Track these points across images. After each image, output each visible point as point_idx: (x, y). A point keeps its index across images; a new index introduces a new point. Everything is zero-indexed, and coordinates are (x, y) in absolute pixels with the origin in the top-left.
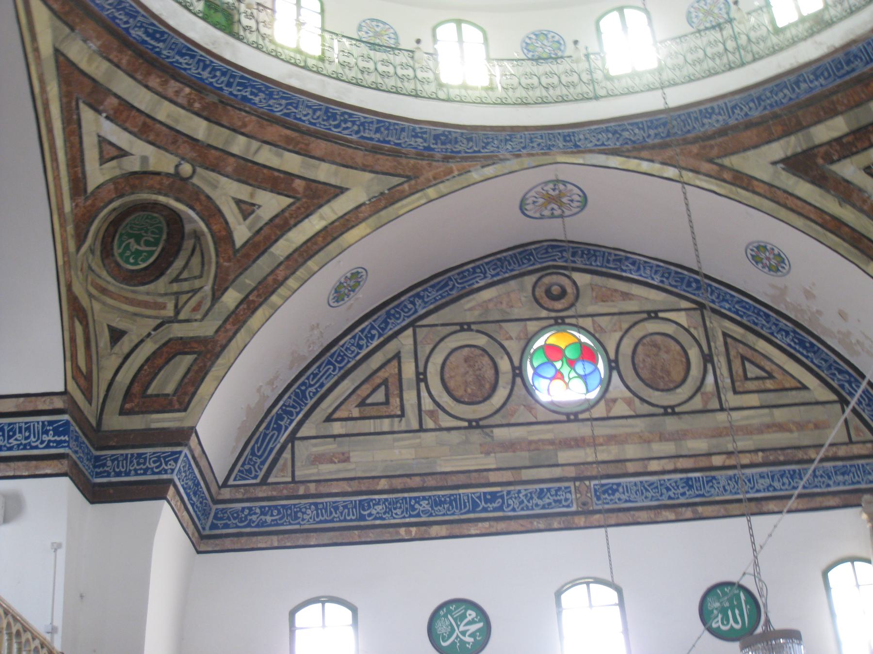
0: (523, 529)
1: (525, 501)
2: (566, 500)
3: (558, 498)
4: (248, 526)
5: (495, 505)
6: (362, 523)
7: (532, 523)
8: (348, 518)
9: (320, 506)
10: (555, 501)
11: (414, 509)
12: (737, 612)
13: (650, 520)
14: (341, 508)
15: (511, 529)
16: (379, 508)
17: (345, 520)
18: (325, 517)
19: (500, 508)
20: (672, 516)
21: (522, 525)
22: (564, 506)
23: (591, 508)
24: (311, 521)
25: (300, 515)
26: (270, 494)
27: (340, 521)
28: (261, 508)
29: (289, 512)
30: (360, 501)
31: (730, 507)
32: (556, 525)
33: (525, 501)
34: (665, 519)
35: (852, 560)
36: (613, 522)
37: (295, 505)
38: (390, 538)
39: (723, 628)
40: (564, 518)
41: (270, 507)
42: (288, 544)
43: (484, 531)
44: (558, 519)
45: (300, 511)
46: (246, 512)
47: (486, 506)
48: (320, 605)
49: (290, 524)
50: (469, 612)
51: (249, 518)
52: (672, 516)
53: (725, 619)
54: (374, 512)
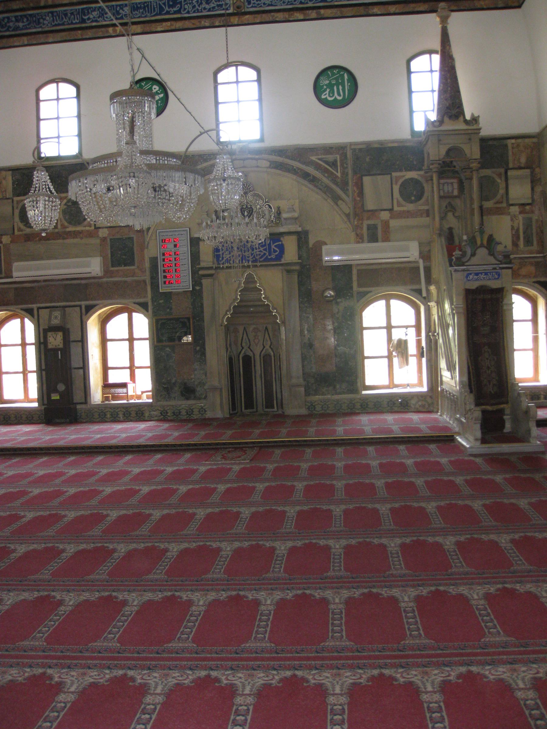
0: (195, 26)
1: (197, 5)
2: (226, 4)
3: (220, 3)
4: (8, 30)
5: (175, 9)
6: (83, 25)
7: (200, 22)
8: (74, 22)
9: (55, 14)
10: (218, 6)
11: (118, 13)
12: (340, 87)
13: (284, 19)
14: (69, 15)
15: (186, 27)
16: (95, 14)
17: (72, 23)
18: (59, 22)
19: (179, 12)
20: (301, 17)
21: (193, 24)
22: (224, 9)
23: (243, 11)
24: (49, 25)
25: (41, 21)
26: (21, 6)
27: (69, 24)
28: (16, 17)
29: (34, 19)
30: (83, 9)
31: (344, 10)
32: (217, 24)
33: (197, 5)
34: (296, 19)
35: (431, 52)
36: (258, 21)
37: (38, 14)
38: (102, 36)
39: (330, 99)
40: (223, 18)
41: (21, 16)
42: (35, 42)
43: (166, 28)
44: (219, 19)
45: (42, 18)
46: (6, 20)
47: (169, 10)
48: (55, 85)
49: (35, 28)
50: (154, 87)
51: (8, 25)
52: (301, 17)
53: (332, 92)
54: (91, 17)
